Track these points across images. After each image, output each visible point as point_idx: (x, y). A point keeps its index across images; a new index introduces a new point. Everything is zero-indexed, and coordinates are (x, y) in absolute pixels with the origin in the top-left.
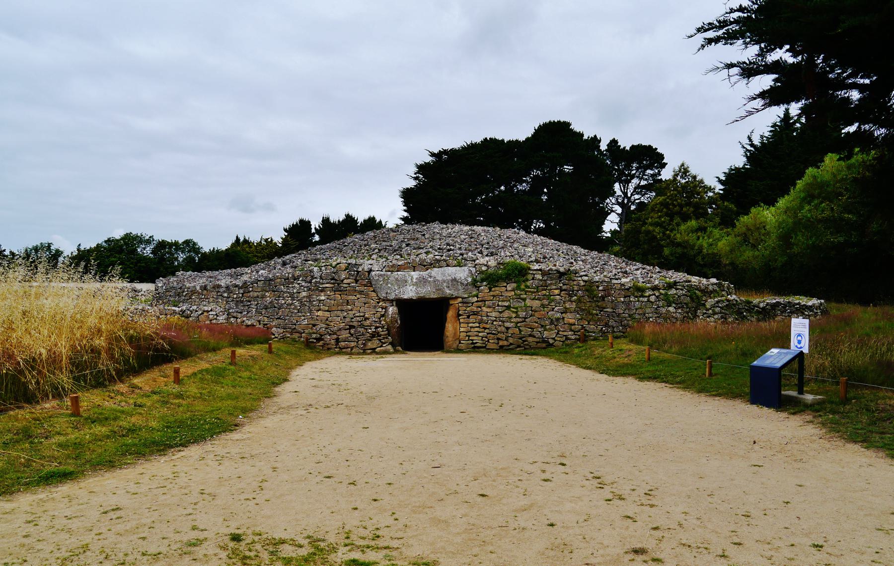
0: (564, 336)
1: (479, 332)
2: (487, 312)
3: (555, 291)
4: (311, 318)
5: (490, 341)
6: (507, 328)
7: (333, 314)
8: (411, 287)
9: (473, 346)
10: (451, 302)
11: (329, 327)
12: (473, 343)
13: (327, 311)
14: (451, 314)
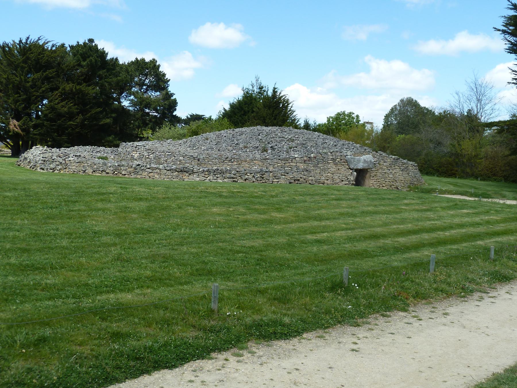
7: (335, 175)
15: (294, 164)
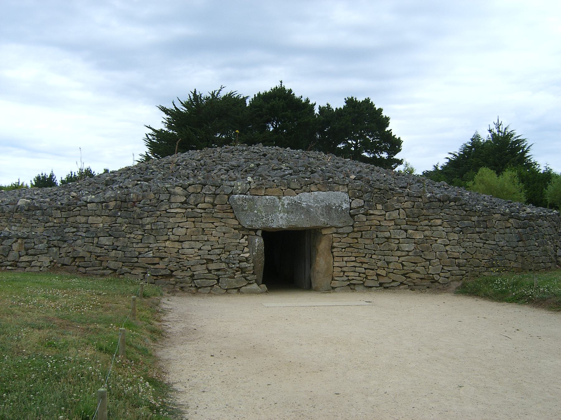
0: (449, 271)
1: (355, 267)
2: (365, 244)
3: (437, 220)
4: (158, 249)
5: (369, 278)
6: (388, 263)
7: (186, 245)
8: (282, 214)
9: (349, 283)
10: (324, 232)
11: (181, 260)
12: (349, 280)
13: (178, 241)
14: (323, 246)
15: (83, 219)
